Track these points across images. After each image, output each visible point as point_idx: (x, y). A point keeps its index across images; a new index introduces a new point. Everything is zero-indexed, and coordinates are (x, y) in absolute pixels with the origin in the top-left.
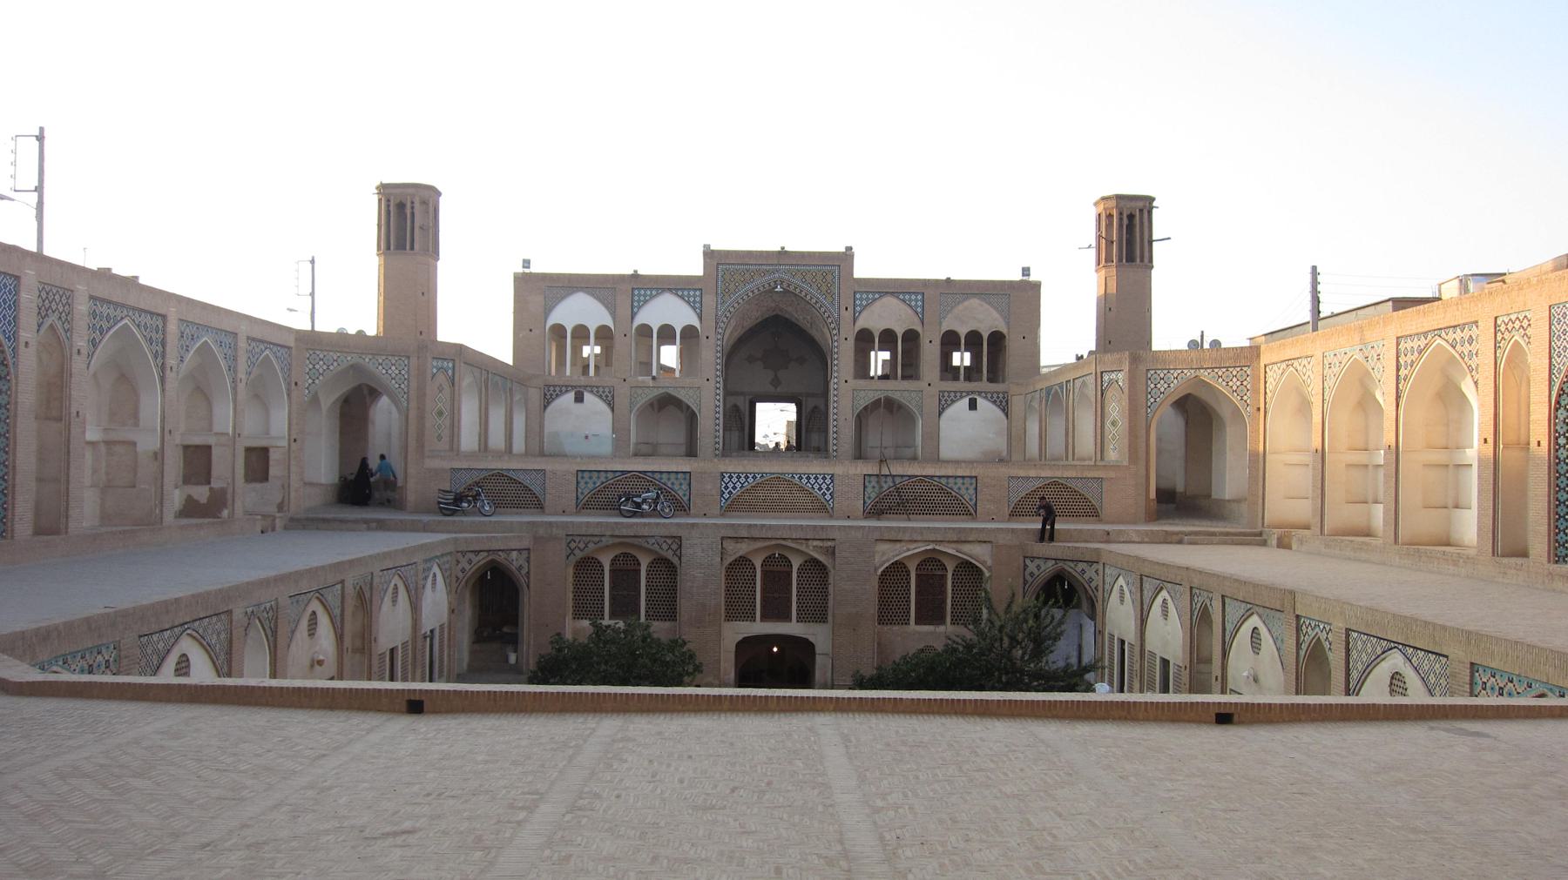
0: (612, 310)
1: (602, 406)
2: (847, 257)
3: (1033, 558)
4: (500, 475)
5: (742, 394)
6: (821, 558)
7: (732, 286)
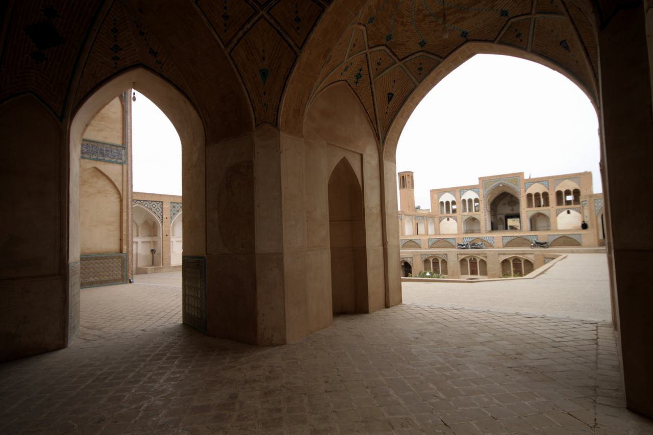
0: (455, 196)
1: (455, 221)
2: (522, 174)
3: (547, 258)
4: (411, 241)
5: (503, 214)
6: (484, 259)
7: (487, 186)
